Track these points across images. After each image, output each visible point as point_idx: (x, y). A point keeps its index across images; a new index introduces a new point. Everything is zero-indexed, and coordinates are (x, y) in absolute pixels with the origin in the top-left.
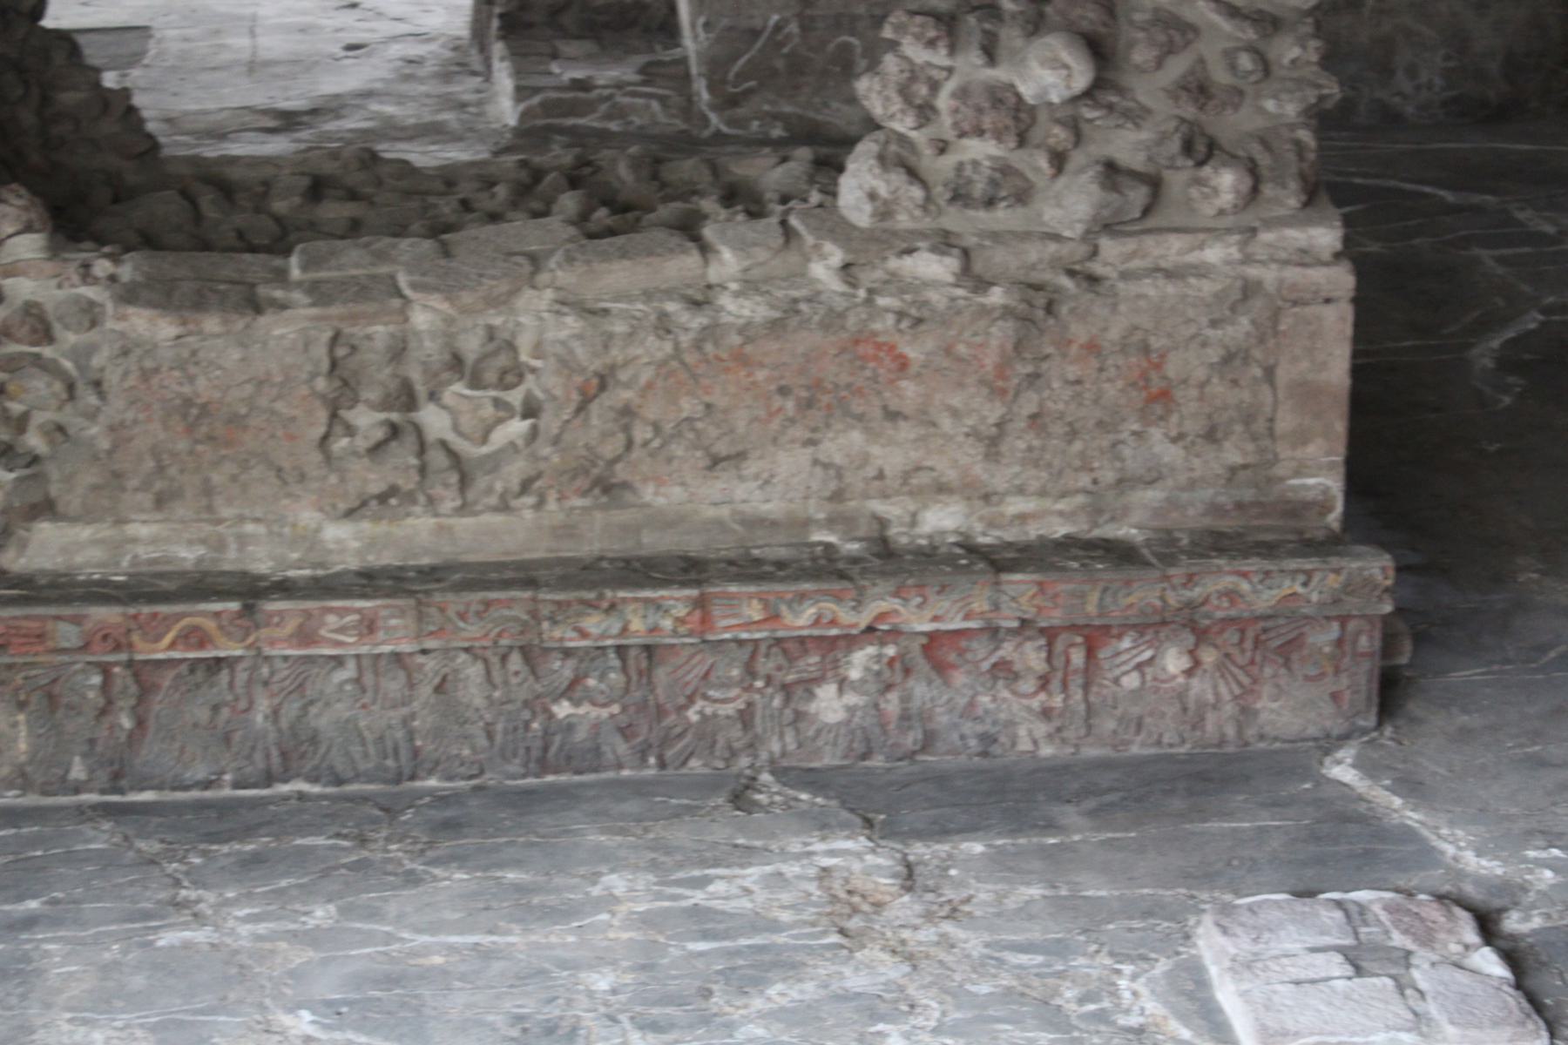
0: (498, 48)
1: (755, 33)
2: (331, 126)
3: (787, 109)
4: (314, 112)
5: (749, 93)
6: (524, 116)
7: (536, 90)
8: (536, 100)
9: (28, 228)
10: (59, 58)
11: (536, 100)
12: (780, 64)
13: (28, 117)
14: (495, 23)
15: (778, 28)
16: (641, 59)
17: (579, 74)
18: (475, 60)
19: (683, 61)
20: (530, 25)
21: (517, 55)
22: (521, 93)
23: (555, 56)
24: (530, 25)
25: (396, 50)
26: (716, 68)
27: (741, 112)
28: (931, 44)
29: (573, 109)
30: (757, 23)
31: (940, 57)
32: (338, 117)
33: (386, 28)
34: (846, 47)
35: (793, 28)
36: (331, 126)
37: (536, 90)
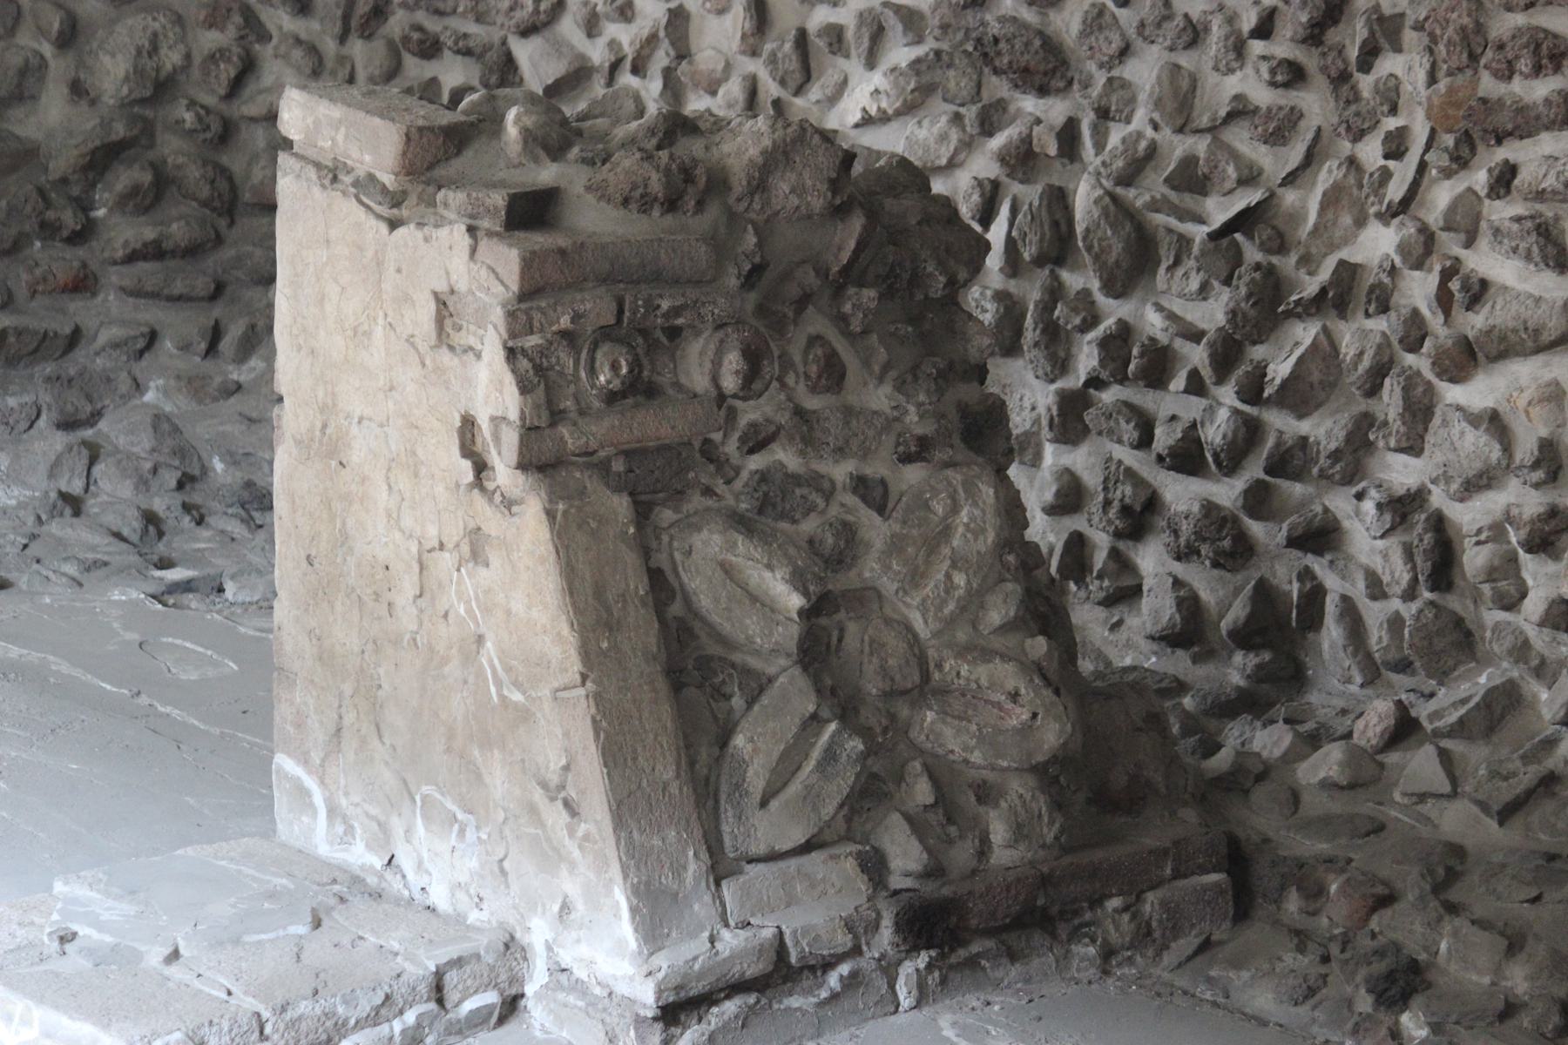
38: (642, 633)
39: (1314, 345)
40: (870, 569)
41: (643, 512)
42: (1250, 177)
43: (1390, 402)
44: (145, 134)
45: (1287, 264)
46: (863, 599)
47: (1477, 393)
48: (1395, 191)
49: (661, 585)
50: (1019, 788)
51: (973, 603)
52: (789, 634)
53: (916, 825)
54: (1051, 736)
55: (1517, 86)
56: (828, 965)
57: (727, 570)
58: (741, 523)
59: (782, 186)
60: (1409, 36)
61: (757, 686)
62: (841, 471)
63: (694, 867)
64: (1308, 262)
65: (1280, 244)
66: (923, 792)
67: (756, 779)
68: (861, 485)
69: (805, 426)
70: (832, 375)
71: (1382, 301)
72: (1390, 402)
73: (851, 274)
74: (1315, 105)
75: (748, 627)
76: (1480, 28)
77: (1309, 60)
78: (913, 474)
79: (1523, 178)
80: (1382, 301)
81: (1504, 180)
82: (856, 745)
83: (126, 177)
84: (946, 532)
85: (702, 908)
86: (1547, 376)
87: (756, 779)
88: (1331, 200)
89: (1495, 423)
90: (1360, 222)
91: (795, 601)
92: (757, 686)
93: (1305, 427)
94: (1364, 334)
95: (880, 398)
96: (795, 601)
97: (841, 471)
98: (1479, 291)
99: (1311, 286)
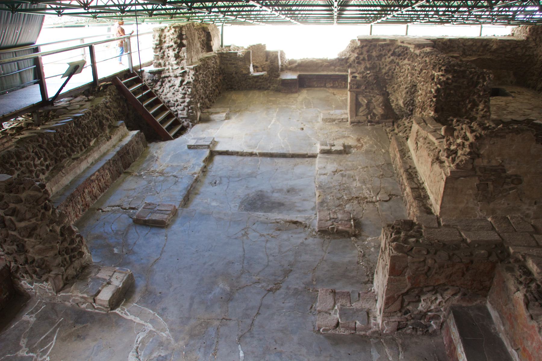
38: (354, 102)
40: (372, 101)
41: (357, 95)
44: (389, 72)
46: (372, 103)
49: (357, 99)
50: (379, 115)
51: (379, 104)
52: (365, 104)
53: (371, 116)
54: (382, 113)
56: (362, 123)
57: (362, 100)
58: (364, 97)
59: (370, 78)
61: (363, 106)
62: (372, 95)
63: (354, 115)
66: (372, 114)
67: (360, 111)
68: (373, 96)
69: (369, 92)
70: (372, 89)
73: (375, 84)
75: (362, 103)
78: (377, 96)
82: (368, 111)
83: (387, 75)
84: (378, 100)
85: (354, 117)
87: (360, 111)
91: (366, 102)
92: (363, 106)
95: (376, 91)
96: (366, 102)
97: (372, 95)
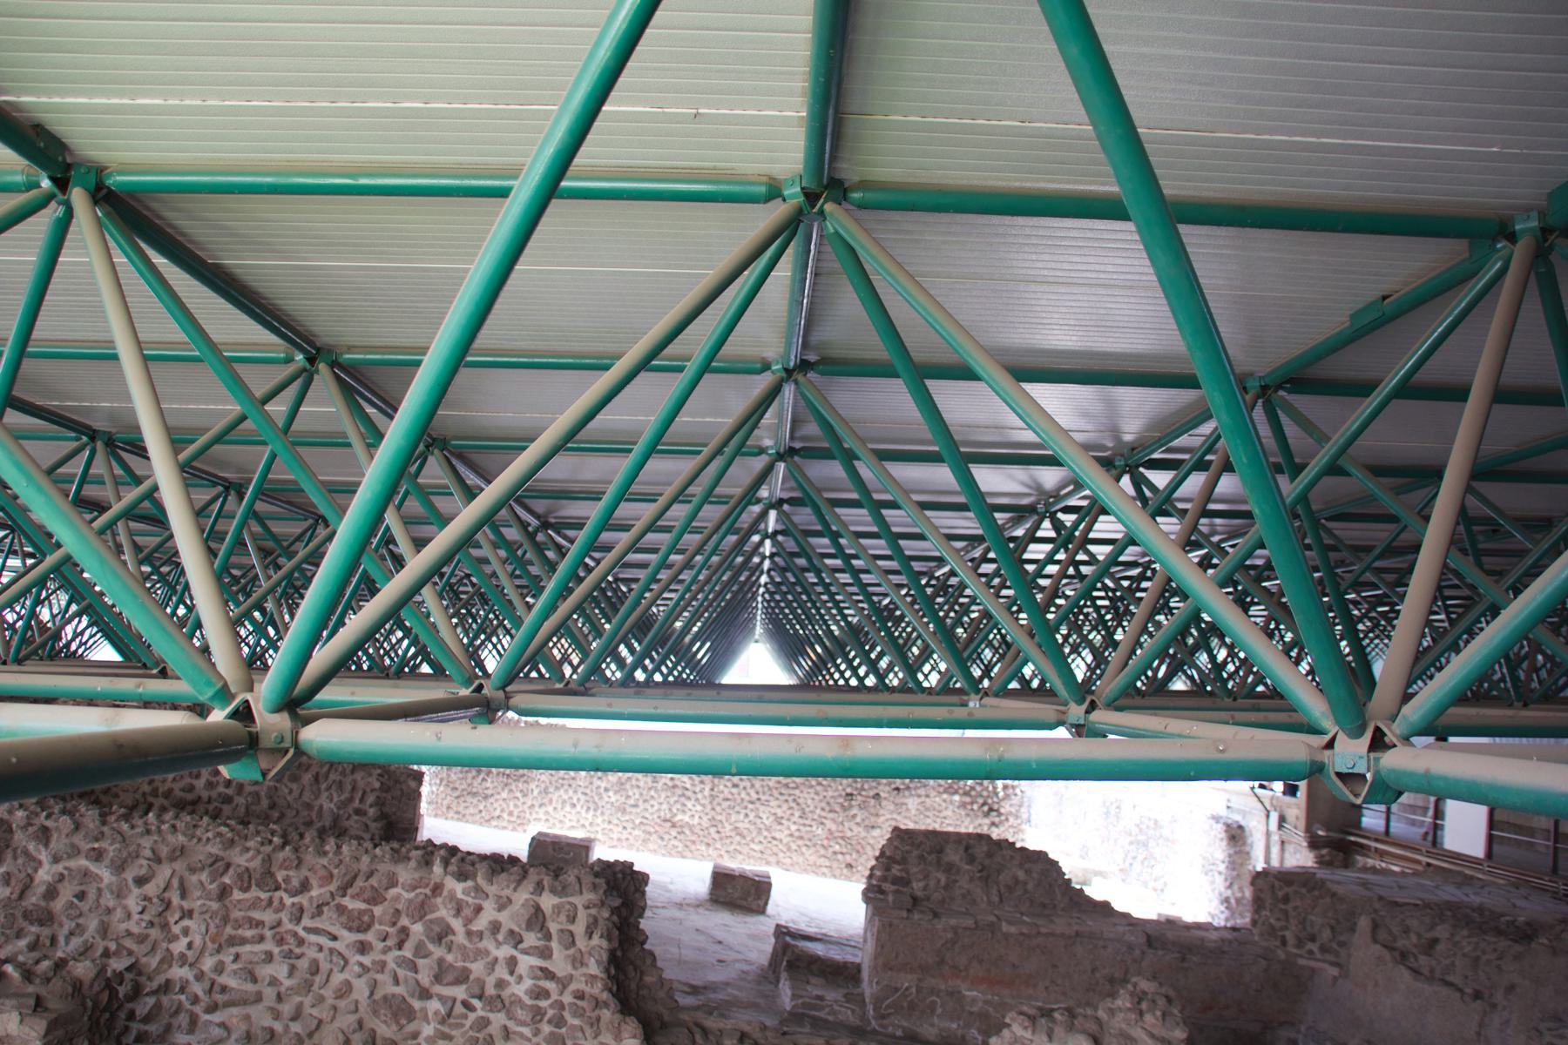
0: (784, 975)
1: (897, 990)
2: (712, 996)
3: (905, 1024)
4: (705, 988)
5: (889, 1014)
6: (794, 1007)
7: (801, 997)
8: (800, 1001)
9: (634, 1037)
10: (649, 962)
11: (800, 1001)
12: (905, 1004)
13: (633, 986)
14: (785, 963)
15: (907, 989)
16: (846, 991)
17: (819, 992)
18: (771, 977)
19: (862, 995)
20: (798, 967)
21: (791, 978)
22: (794, 997)
23: (808, 983)
24: (798, 967)
25: (739, 966)
26: (878, 1001)
27: (885, 1022)
28: (1026, 1028)
29: (814, 1007)
30: (899, 985)
31: (1028, 1034)
32: (715, 992)
33: (734, 956)
34: (934, 1002)
35: (914, 990)
36: (712, 996)
37: (801, 997)
39: (155, 1005)
42: (130, 953)
43: (183, 1019)
45: (143, 979)
47: (217, 1017)
48: (191, 959)
55: (240, 932)
60: (196, 915)
64: (150, 979)
65: (140, 973)
71: (182, 990)
72: (183, 1019)
74: (154, 933)
76: (228, 916)
77: (156, 920)
79: (244, 958)
80: (182, 990)
81: (237, 957)
86: (244, 1012)
88: (162, 961)
89: (223, 1025)
90: (170, 966)
93: (147, 1028)
94: (172, 1000)
98: (224, 989)
99: (154, 985)
